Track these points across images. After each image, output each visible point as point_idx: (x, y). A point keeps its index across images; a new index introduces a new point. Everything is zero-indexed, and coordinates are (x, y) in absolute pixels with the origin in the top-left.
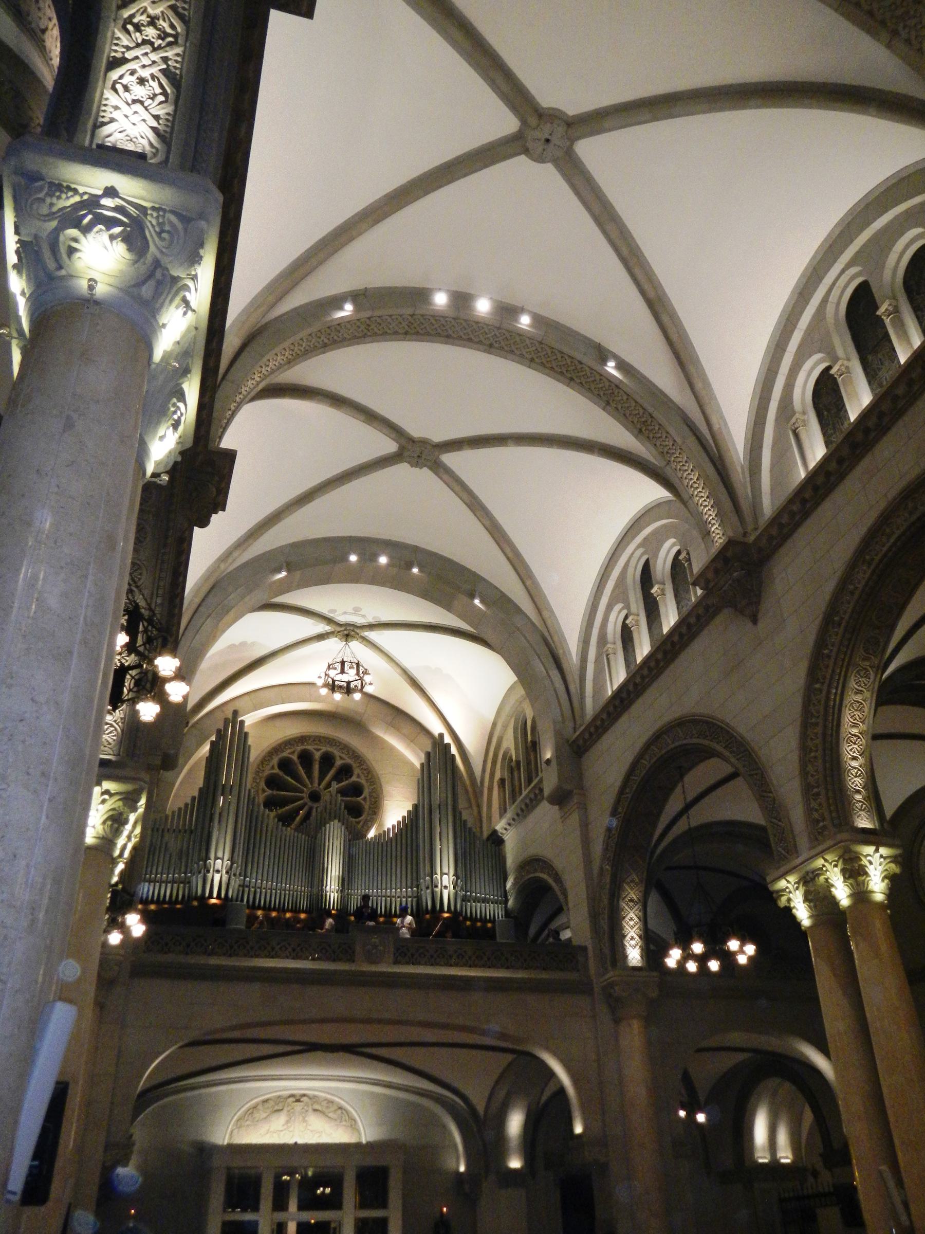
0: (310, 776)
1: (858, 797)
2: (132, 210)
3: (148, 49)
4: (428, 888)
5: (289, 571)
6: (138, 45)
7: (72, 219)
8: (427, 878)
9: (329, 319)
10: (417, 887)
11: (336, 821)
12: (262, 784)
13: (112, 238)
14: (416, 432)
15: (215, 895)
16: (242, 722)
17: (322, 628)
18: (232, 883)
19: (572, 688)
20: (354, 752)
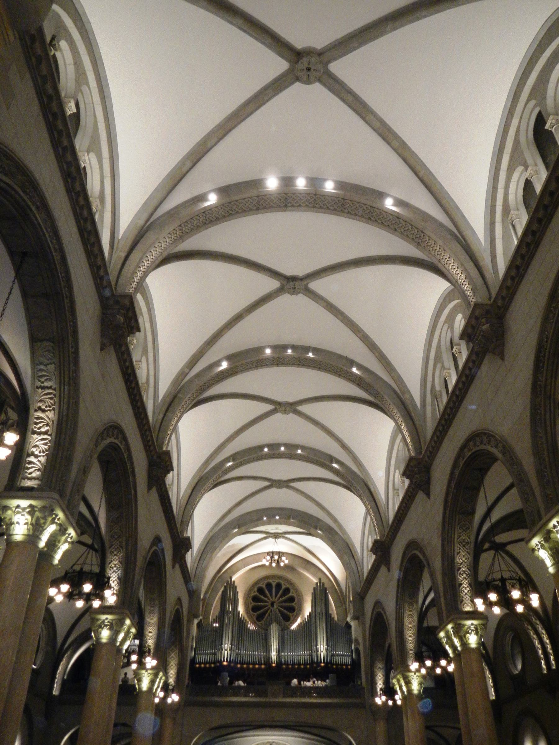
0: (271, 594)
1: (411, 652)
2: (111, 621)
3: (114, 573)
4: (315, 652)
5: (239, 527)
6: (113, 573)
7: (100, 627)
8: (315, 647)
9: (224, 468)
10: (312, 651)
11: (275, 623)
12: (250, 600)
13: (107, 629)
14: (276, 478)
15: (225, 660)
16: (234, 582)
17: (264, 535)
18: (232, 655)
19: (359, 568)
20: (290, 581)
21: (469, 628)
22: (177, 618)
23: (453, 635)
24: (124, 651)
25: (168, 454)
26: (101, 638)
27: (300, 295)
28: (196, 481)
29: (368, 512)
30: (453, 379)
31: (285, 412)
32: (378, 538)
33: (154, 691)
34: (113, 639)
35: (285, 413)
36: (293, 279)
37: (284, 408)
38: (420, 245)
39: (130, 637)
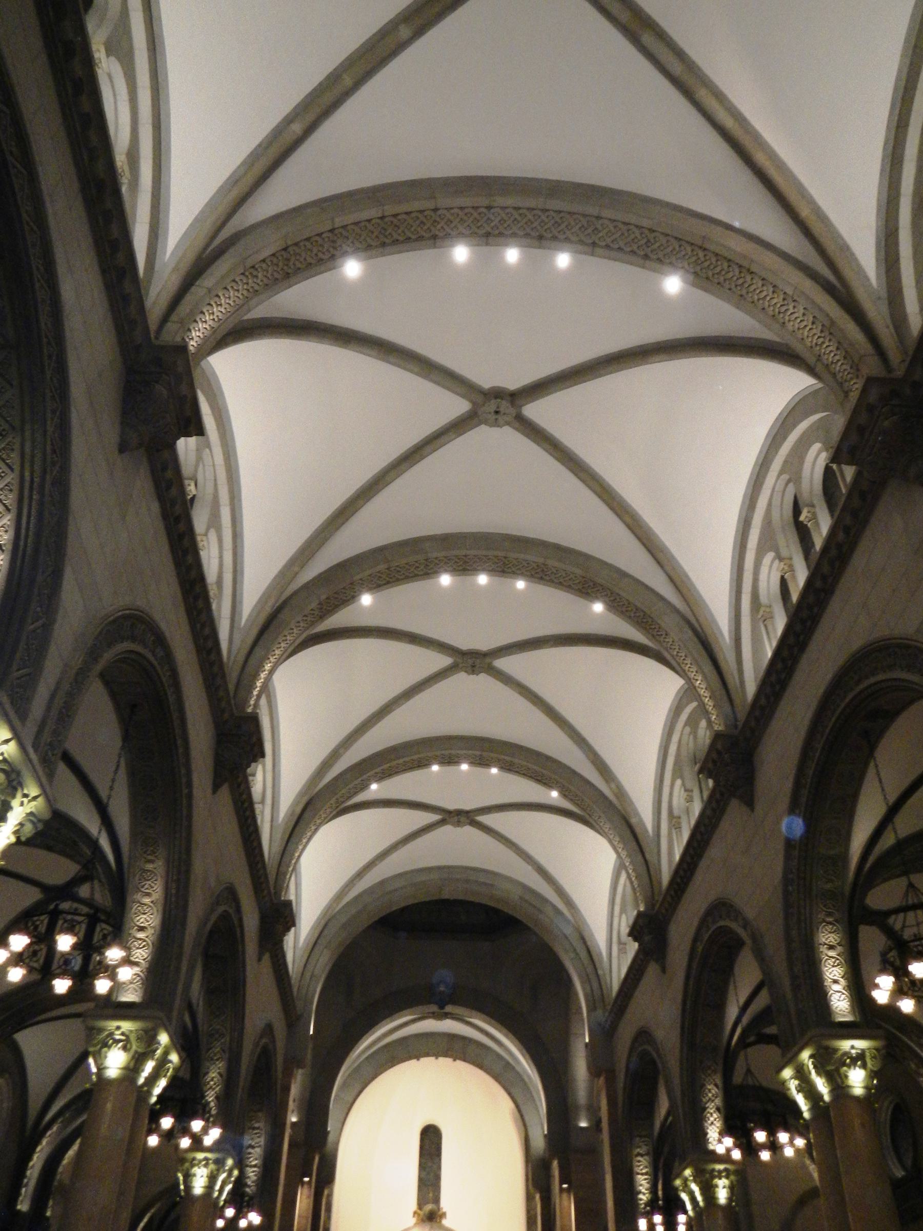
2: (127, 1033)
7: (106, 1045)
13: (119, 1048)
14: (451, 806)
21: (846, 1054)
22: (265, 1057)
23: (813, 1072)
24: (154, 1099)
25: (254, 720)
26: (105, 1068)
27: (507, 430)
28: (305, 800)
29: (620, 868)
30: (801, 575)
31: (473, 670)
32: (642, 909)
33: (216, 1194)
34: (132, 1069)
35: (473, 672)
36: (498, 394)
37: (470, 661)
38: (745, 299)
39: (168, 1069)
